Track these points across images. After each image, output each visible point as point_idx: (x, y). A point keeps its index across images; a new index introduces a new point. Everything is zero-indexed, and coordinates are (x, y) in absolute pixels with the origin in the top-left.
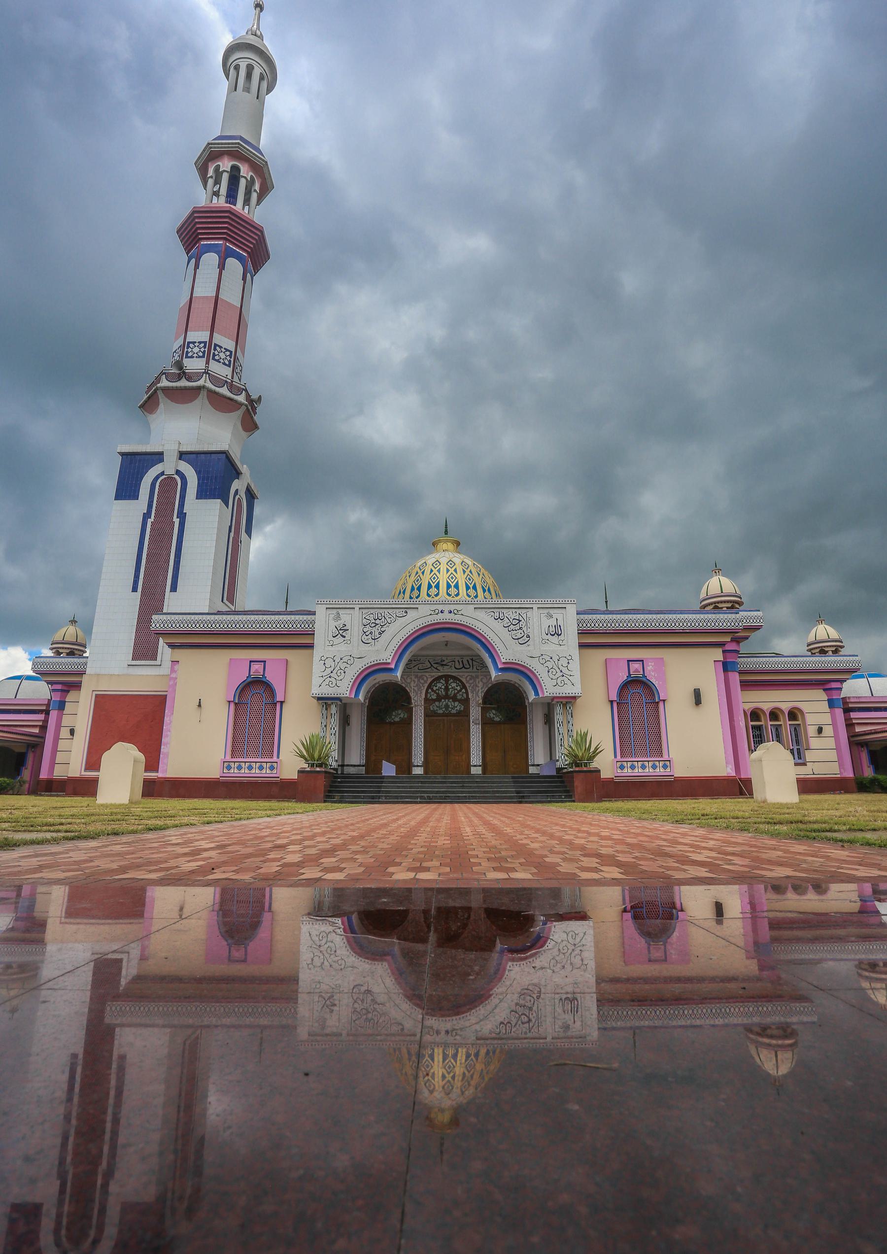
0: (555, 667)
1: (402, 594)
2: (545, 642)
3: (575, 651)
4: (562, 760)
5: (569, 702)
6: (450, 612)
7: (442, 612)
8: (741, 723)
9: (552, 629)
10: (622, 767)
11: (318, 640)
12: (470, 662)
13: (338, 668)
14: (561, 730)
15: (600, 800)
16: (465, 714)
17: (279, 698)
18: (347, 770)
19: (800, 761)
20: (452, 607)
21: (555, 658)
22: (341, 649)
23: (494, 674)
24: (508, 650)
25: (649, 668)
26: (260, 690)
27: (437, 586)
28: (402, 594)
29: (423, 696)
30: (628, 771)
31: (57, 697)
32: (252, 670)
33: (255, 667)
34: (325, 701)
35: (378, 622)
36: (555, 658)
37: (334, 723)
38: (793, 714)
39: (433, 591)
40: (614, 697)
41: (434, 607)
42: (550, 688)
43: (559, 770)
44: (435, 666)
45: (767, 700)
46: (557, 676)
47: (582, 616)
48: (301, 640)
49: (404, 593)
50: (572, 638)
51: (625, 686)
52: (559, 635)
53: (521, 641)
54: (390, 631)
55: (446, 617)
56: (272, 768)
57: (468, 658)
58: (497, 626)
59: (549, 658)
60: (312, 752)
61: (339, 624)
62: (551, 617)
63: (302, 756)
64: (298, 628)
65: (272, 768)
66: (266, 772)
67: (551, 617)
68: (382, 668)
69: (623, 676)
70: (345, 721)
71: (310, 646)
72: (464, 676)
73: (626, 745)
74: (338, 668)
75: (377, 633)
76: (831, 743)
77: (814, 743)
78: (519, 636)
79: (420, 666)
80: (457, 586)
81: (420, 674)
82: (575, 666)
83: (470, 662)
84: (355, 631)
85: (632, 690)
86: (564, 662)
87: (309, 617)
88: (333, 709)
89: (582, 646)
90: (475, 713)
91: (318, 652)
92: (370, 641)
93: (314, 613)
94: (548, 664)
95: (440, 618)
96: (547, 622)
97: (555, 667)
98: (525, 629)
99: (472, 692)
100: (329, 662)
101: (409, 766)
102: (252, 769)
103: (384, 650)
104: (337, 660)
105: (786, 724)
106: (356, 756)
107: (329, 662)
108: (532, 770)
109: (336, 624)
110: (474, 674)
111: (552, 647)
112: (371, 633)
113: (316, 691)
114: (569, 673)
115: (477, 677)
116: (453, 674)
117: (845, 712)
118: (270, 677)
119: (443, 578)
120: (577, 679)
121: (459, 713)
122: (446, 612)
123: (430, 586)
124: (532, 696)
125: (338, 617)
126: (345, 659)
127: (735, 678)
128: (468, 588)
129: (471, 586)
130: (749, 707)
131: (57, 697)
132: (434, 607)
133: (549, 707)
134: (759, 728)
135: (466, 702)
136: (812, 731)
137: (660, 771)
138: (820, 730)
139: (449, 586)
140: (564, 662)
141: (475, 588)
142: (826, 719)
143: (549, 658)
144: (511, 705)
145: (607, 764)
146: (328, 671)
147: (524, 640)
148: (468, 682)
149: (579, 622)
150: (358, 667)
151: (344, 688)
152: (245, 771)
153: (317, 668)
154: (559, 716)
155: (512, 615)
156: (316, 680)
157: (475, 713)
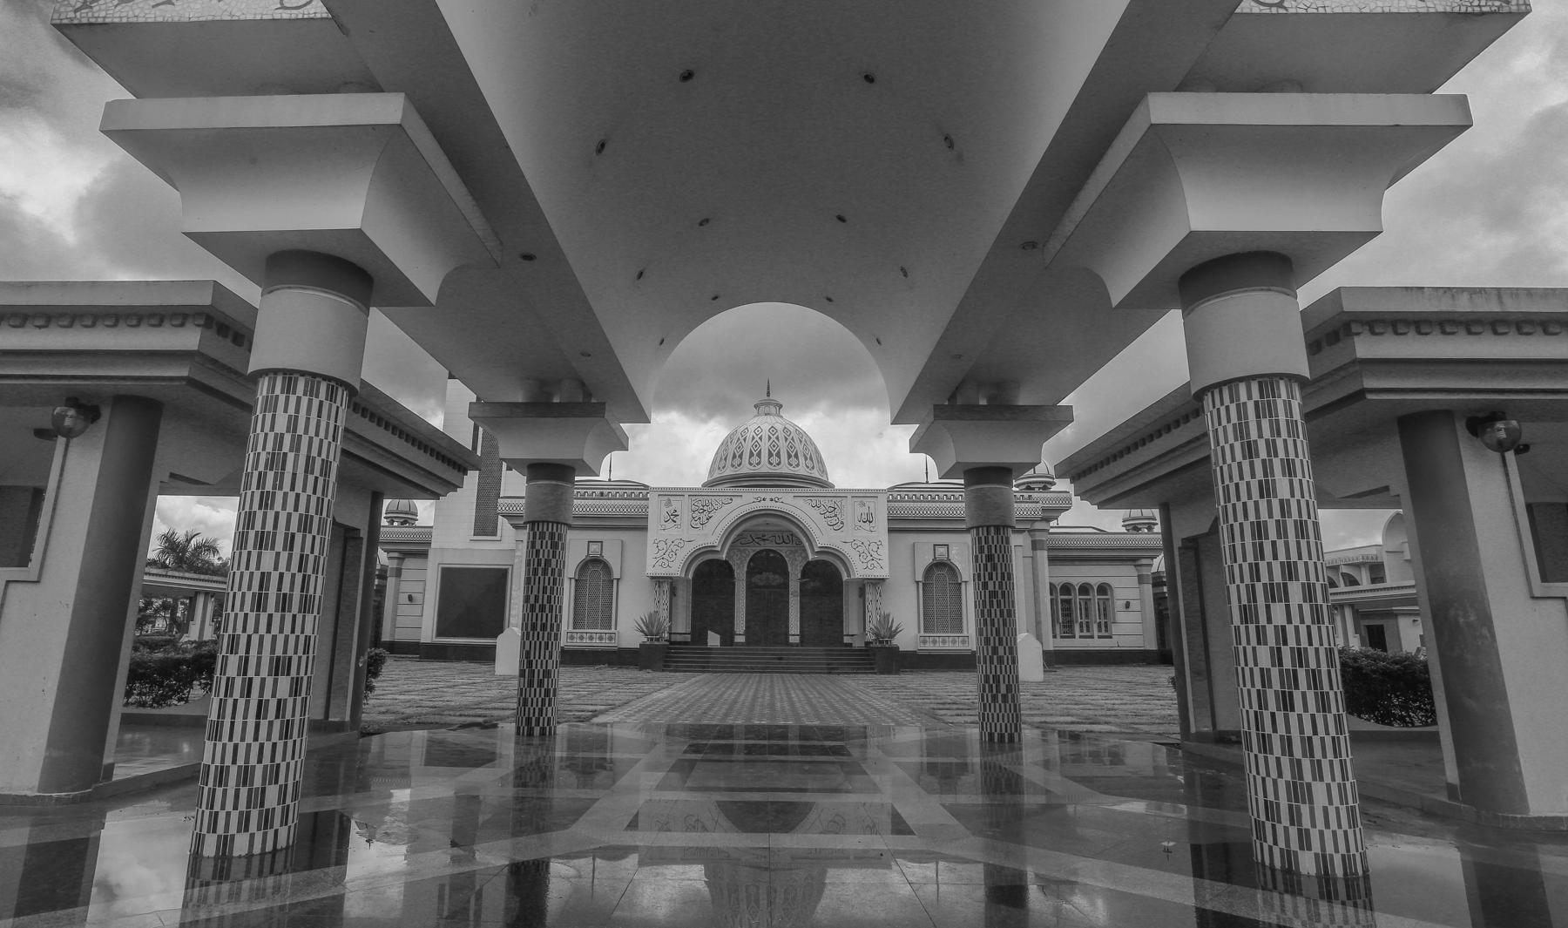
2: (857, 528)
3: (883, 535)
4: (870, 637)
5: (878, 582)
8: (1046, 597)
10: (925, 642)
11: (652, 524)
14: (870, 607)
15: (897, 672)
16: (786, 586)
17: (616, 575)
18: (674, 638)
19: (1103, 633)
20: (773, 496)
22: (673, 533)
23: (811, 557)
24: (823, 536)
26: (599, 568)
27: (759, 455)
30: (929, 646)
31: (393, 564)
33: (594, 547)
34: (658, 580)
37: (666, 598)
38: (1103, 589)
39: (755, 459)
40: (920, 577)
42: (860, 570)
43: (867, 643)
45: (1077, 575)
48: (637, 524)
50: (882, 524)
51: (929, 570)
54: (717, 516)
55: (768, 504)
56: (611, 639)
58: (814, 513)
60: (650, 627)
61: (671, 510)
64: (633, 512)
65: (611, 639)
66: (605, 643)
68: (709, 550)
69: (929, 560)
70: (673, 592)
71: (645, 528)
72: (784, 551)
73: (929, 621)
76: (1136, 617)
77: (1121, 616)
80: (778, 455)
82: (884, 551)
84: (685, 518)
85: (937, 572)
88: (666, 587)
89: (891, 531)
90: (794, 585)
91: (652, 533)
95: (762, 505)
96: (860, 510)
100: (662, 545)
101: (732, 634)
102: (592, 639)
103: (712, 535)
105: (1095, 597)
106: (683, 626)
107: (662, 545)
108: (846, 640)
111: (863, 534)
113: (650, 571)
117: (1155, 585)
118: (607, 556)
119: (765, 447)
120: (885, 562)
121: (779, 586)
123: (751, 454)
124: (845, 577)
125: (669, 503)
127: (1043, 555)
128: (789, 456)
130: (1059, 582)
131: (393, 564)
133: (864, 586)
134: (1069, 602)
135: (785, 574)
136: (1119, 605)
137: (959, 646)
138: (1128, 605)
139: (770, 455)
141: (796, 456)
142: (1132, 594)
144: (826, 579)
145: (908, 637)
147: (838, 526)
150: (689, 549)
151: (675, 568)
152: (586, 642)
153: (651, 550)
154: (869, 597)
155: (827, 503)
156: (650, 561)
157: (794, 585)
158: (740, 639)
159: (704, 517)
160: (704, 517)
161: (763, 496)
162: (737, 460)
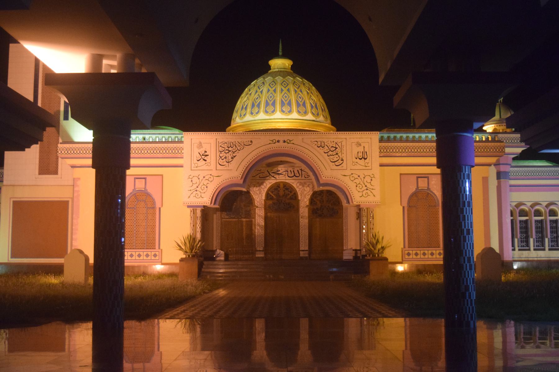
0: (361, 183)
1: (244, 109)
6: (284, 142)
7: (278, 141)
8: (508, 220)
9: (360, 155)
12: (300, 171)
13: (202, 184)
17: (158, 205)
21: (362, 176)
25: (433, 182)
28: (244, 109)
29: (264, 198)
32: (137, 186)
35: (230, 149)
36: (362, 176)
40: (405, 204)
41: (272, 138)
44: (273, 174)
46: (363, 189)
47: (383, 144)
49: (246, 108)
52: (365, 159)
53: (337, 163)
54: (240, 155)
57: (298, 169)
59: (357, 177)
61: (202, 151)
62: (360, 145)
63: (181, 249)
67: (360, 145)
69: (413, 189)
74: (202, 184)
75: (230, 158)
78: (336, 159)
79: (261, 175)
81: (261, 181)
82: (376, 183)
83: (300, 171)
86: (368, 179)
87: (178, 145)
92: (225, 163)
93: (182, 142)
94: (356, 181)
96: (356, 149)
97: (361, 183)
98: (340, 154)
99: (301, 195)
104: (201, 178)
107: (195, 180)
109: (199, 151)
110: (302, 181)
112: (225, 158)
114: (372, 187)
115: (305, 183)
116: (287, 181)
118: (150, 190)
120: (377, 192)
122: (281, 142)
126: (207, 177)
129: (301, 103)
132: (272, 138)
140: (368, 179)
143: (357, 177)
146: (195, 186)
147: (339, 163)
148: (298, 187)
149: (380, 148)
158: (260, 255)
159: (229, 156)
160: (229, 156)
161: (277, 138)
162: (256, 109)
